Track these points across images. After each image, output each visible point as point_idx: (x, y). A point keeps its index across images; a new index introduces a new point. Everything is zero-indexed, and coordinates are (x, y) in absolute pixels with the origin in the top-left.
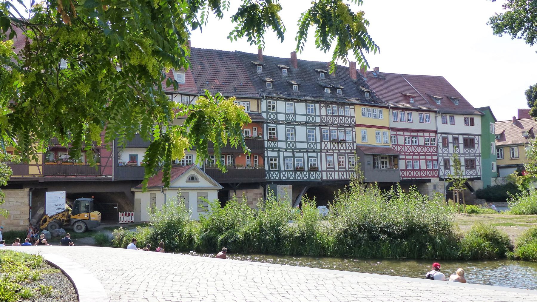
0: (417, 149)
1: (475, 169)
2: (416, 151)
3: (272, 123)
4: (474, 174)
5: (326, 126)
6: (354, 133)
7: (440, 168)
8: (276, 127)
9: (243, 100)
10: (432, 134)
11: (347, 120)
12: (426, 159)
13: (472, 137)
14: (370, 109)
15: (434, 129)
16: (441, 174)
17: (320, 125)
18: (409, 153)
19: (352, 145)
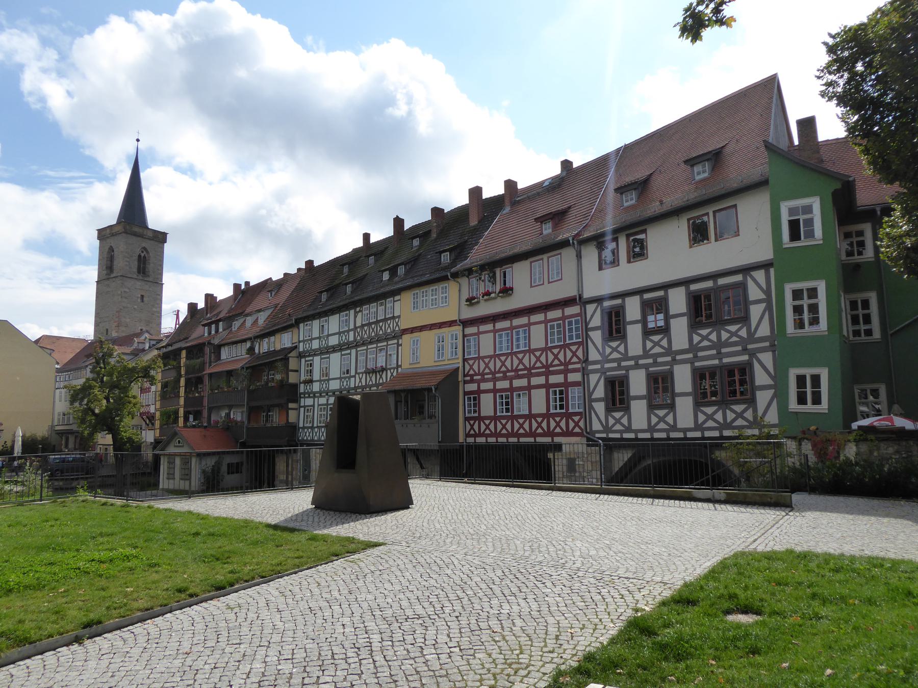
0: (526, 361)
1: (751, 402)
2: (521, 367)
3: (309, 356)
4: (740, 422)
5: (363, 344)
6: (400, 348)
7: (591, 407)
8: (313, 360)
9: (288, 331)
10: (570, 311)
11: (389, 326)
12: (547, 386)
13: (738, 278)
14: (426, 292)
15: (572, 292)
16: (596, 426)
17: (356, 345)
18: (504, 373)
19: (395, 374)
